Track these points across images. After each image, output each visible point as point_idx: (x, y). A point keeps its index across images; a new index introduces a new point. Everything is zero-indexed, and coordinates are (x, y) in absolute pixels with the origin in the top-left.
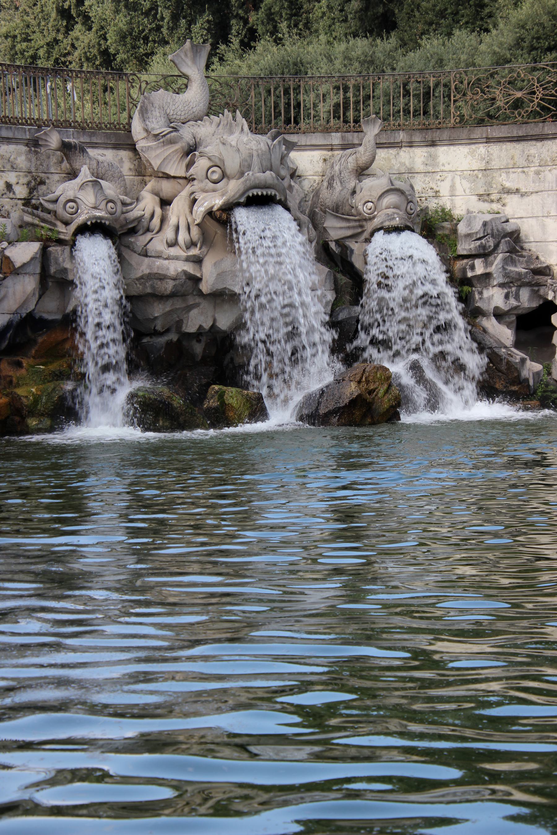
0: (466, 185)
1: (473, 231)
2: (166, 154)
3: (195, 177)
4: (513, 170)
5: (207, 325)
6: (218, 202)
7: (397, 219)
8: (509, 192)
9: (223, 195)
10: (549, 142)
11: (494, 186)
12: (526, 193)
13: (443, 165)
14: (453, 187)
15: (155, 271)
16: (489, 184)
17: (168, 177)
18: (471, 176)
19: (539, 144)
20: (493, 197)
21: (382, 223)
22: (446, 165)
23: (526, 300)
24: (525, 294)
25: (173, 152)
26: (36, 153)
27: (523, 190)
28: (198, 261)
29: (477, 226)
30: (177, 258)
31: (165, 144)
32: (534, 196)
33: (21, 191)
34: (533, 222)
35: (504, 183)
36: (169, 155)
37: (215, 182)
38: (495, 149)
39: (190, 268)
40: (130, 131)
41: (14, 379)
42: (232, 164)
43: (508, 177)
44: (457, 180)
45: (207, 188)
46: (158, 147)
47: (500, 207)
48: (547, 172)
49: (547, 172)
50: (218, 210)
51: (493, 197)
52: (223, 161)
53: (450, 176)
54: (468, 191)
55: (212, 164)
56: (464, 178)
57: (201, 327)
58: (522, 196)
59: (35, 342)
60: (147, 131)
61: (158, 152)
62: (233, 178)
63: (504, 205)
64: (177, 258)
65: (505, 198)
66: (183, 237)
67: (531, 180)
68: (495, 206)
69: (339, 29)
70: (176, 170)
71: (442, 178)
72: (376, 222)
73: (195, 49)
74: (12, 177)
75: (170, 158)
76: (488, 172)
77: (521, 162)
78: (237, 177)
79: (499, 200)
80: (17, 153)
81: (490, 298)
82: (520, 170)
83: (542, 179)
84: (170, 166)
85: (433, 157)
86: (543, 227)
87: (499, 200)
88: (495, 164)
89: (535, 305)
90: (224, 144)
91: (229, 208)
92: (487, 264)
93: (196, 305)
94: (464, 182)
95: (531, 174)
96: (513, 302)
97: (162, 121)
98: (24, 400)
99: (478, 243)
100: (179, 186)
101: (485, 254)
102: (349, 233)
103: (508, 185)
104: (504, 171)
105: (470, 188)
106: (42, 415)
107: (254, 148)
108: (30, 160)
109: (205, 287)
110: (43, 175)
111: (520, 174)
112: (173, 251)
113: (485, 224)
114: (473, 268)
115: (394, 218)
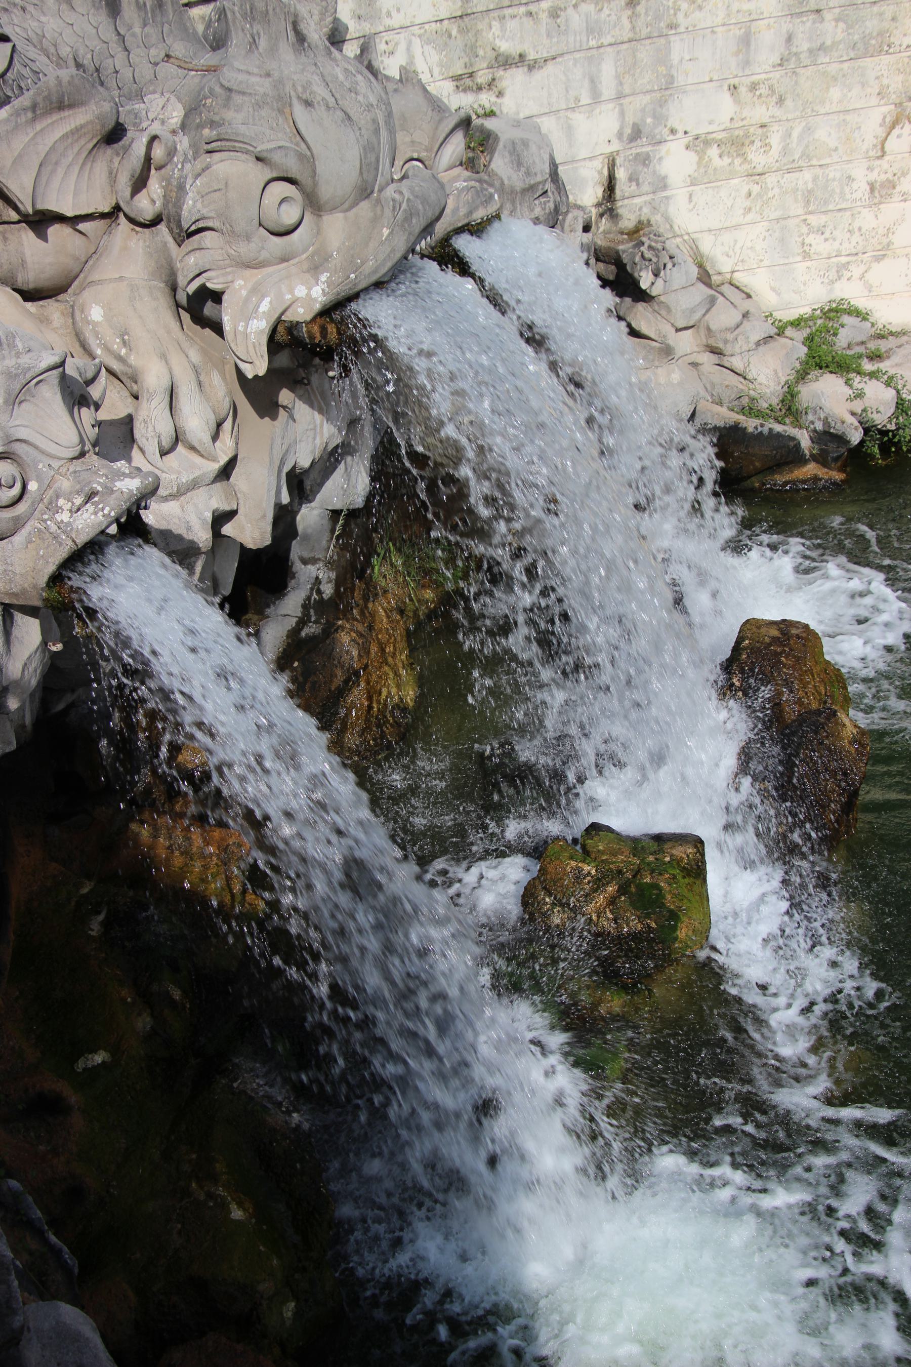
0: (434, 57)
1: (539, 178)
2: (43, 148)
3: (210, 224)
6: (306, 297)
7: (496, 196)
8: (505, 62)
9: (315, 269)
11: (481, 53)
12: (535, 61)
13: (389, 15)
16: (472, 50)
17: (40, 221)
21: (470, 213)
22: (394, 13)
25: (65, 137)
27: (532, 56)
32: (550, 67)
36: (53, 149)
45: (264, 255)
46: (17, 127)
47: (493, 99)
48: (570, 11)
49: (570, 11)
50: (314, 319)
51: (482, 78)
52: (308, 160)
53: (402, 37)
54: (436, 71)
55: (269, 176)
56: (429, 42)
58: (531, 68)
61: (19, 142)
62: (334, 209)
63: (500, 94)
65: (501, 78)
67: (543, 30)
68: (486, 99)
70: (75, 194)
71: (390, 48)
76: (466, 19)
78: (346, 205)
79: (491, 84)
82: (522, 10)
83: (563, 28)
86: (569, 130)
90: (308, 104)
95: (544, 16)
103: (504, 46)
104: (495, 14)
105: (441, 64)
107: (373, 99)
111: (525, 19)
115: (491, 196)
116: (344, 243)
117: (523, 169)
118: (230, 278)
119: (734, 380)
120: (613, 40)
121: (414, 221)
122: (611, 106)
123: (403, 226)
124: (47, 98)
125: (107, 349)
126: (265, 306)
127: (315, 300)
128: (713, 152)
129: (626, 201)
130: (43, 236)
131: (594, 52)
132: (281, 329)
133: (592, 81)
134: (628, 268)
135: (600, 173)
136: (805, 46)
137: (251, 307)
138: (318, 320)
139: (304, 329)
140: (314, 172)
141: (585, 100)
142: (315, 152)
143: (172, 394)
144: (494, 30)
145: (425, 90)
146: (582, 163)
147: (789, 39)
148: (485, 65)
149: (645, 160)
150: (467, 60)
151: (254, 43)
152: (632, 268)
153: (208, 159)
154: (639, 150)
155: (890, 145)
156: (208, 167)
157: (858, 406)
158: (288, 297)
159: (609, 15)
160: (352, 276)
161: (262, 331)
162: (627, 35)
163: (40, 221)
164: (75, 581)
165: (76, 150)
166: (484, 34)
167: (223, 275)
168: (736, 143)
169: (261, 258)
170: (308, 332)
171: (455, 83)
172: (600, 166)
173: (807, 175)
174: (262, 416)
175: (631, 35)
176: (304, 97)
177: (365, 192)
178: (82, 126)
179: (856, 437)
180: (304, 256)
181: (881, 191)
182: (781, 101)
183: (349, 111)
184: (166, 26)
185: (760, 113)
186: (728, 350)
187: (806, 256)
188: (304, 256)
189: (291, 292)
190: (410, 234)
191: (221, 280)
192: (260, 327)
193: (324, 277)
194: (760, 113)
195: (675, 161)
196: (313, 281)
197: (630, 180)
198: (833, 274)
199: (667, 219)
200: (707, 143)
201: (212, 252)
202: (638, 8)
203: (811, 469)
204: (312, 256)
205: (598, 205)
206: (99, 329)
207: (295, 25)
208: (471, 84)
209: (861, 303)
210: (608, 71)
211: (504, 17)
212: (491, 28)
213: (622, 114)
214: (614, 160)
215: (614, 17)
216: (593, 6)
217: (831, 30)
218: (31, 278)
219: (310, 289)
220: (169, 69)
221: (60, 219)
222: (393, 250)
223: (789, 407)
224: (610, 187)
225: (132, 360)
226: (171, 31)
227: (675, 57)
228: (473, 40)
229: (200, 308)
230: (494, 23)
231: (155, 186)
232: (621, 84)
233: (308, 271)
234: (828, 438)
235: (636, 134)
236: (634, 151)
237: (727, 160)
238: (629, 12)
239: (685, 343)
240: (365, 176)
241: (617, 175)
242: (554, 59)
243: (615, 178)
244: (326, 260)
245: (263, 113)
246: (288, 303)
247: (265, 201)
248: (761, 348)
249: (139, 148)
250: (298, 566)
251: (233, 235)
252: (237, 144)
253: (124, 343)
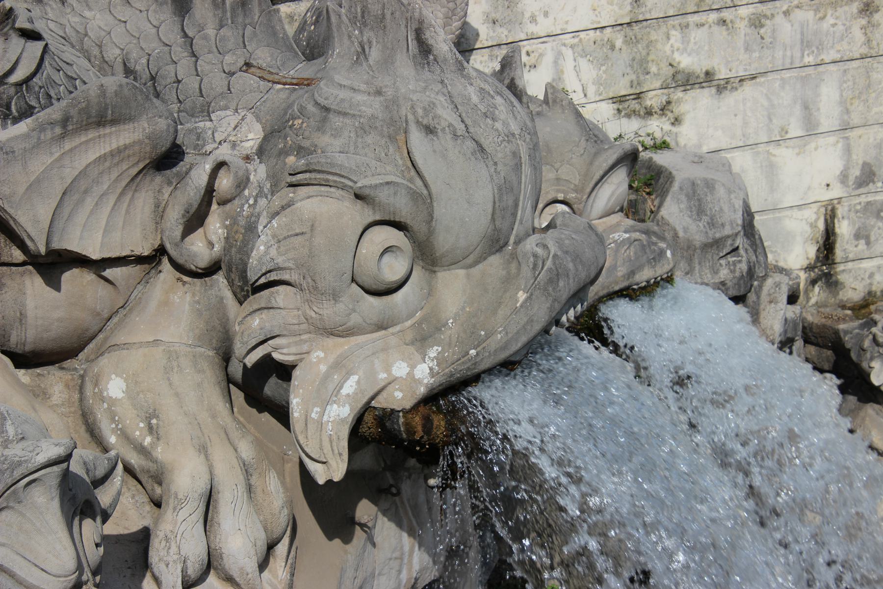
0: (589, 72)
1: (727, 231)
2: (70, 173)
3: (286, 277)
4: (696, 18)
6: (407, 375)
8: (686, 81)
9: (421, 341)
11: (653, 69)
12: (727, 81)
13: (533, 19)
16: (641, 66)
17: (53, 264)
18: (599, 42)
20: (653, 100)
21: (632, 273)
22: (540, 18)
25: (102, 159)
27: (722, 73)
31: (67, 126)
32: (748, 89)
35: (676, 56)
36: (83, 173)
43: (685, 40)
46: (38, 145)
47: (667, 127)
48: (779, 19)
49: (779, 19)
50: (415, 407)
51: (653, 100)
52: (424, 200)
53: (548, 49)
54: (591, 90)
55: (371, 219)
56: (584, 54)
58: (720, 89)
61: (39, 164)
62: (454, 263)
63: (677, 121)
65: (679, 101)
67: (740, 43)
68: (657, 127)
75: (83, 185)
76: (636, 27)
79: (664, 109)
82: (713, 16)
83: (768, 40)
84: (81, 217)
86: (771, 169)
90: (429, 130)
94: (583, 63)
95: (742, 26)
100: (103, 290)
103: (685, 62)
105: (598, 82)
107: (514, 127)
111: (716, 29)
115: (662, 253)
116: (463, 308)
117: (705, 219)
118: (305, 348)
120: (838, 57)
121: (561, 284)
122: (832, 139)
123: (545, 289)
124: (85, 111)
125: (125, 436)
126: (350, 387)
127: (419, 382)
129: (850, 265)
130: (54, 283)
131: (810, 71)
132: (369, 418)
133: (806, 107)
134: (853, 355)
135: (813, 226)
137: (331, 387)
138: (421, 409)
139: (401, 420)
140: (431, 216)
141: (795, 131)
142: (434, 190)
143: (209, 500)
144: (672, 41)
145: (579, 115)
146: (788, 213)
148: (658, 84)
150: (634, 77)
151: (363, 53)
152: (859, 356)
153: (290, 194)
154: (870, 198)
156: (289, 205)
158: (383, 376)
159: (834, 25)
160: (473, 352)
161: (343, 421)
162: (858, 49)
163: (53, 264)
165: (115, 174)
166: (659, 46)
167: (296, 343)
169: (349, 324)
170: (407, 424)
171: (616, 106)
172: (814, 217)
174: (330, 536)
175: (864, 50)
176: (425, 122)
177: (496, 243)
178: (126, 147)
180: (409, 323)
183: (482, 141)
184: (249, 29)
188: (409, 323)
189: (388, 369)
190: (555, 300)
191: (293, 350)
192: (340, 413)
193: (433, 352)
196: (418, 356)
197: (857, 236)
201: (283, 312)
202: (877, 17)
204: (419, 323)
205: (809, 268)
206: (118, 409)
207: (419, 34)
208: (637, 107)
211: (687, 26)
212: (668, 38)
213: (848, 150)
214: (833, 210)
215: (841, 28)
216: (809, 15)
218: (27, 337)
219: (413, 367)
220: (250, 80)
221: (81, 261)
222: (531, 321)
224: (828, 244)
225: (159, 452)
226: (255, 34)
228: (644, 53)
229: (261, 386)
230: (673, 32)
231: (215, 226)
232: (848, 112)
233: (412, 343)
235: (868, 177)
236: (864, 199)
238: (864, 22)
240: (498, 223)
241: (837, 230)
242: (753, 78)
243: (834, 234)
244: (438, 329)
245: (369, 139)
246: (383, 384)
247: (363, 249)
249: (200, 177)
251: (313, 290)
252: (331, 177)
253: (150, 428)
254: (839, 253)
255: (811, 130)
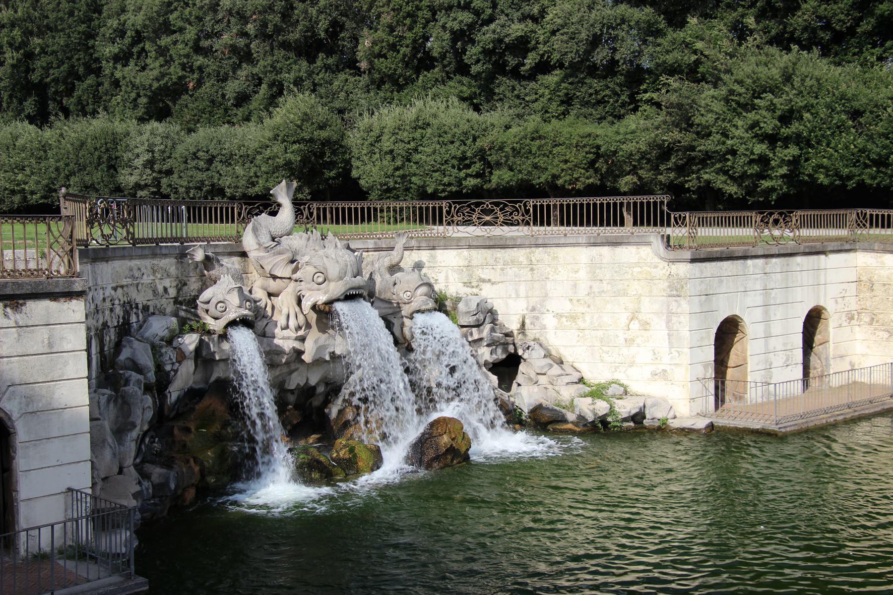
0: (456, 276)
5: (302, 384)
6: (322, 298)
8: (484, 281)
9: (325, 293)
10: (509, 251)
14: (447, 277)
15: (274, 348)
16: (471, 276)
17: (275, 277)
18: (459, 270)
19: (503, 251)
20: (473, 284)
23: (500, 355)
24: (499, 351)
26: (182, 262)
27: (493, 280)
28: (302, 339)
29: (473, 307)
30: (288, 338)
33: (172, 292)
34: (499, 301)
37: (319, 284)
38: (474, 252)
39: (297, 345)
40: (241, 241)
41: (188, 443)
42: (333, 271)
44: (450, 272)
51: (474, 284)
52: (326, 269)
57: (298, 384)
59: (193, 409)
60: (259, 244)
64: (288, 338)
66: (292, 323)
68: (475, 290)
69: (128, 113)
72: (414, 306)
73: (288, 186)
74: (167, 283)
77: (491, 262)
79: (477, 287)
80: (169, 264)
81: (483, 354)
85: (433, 257)
87: (477, 287)
88: (474, 263)
89: (504, 356)
91: (330, 303)
92: (480, 332)
93: (296, 370)
95: (499, 270)
96: (495, 356)
97: (269, 237)
98: (206, 463)
99: (475, 318)
101: (478, 326)
102: (390, 311)
103: (483, 276)
106: (219, 473)
108: (177, 269)
109: (307, 358)
110: (185, 279)
112: (286, 333)
113: (478, 305)
114: (471, 334)
119: (555, 394)
128: (564, 319)
136: (597, 290)
147: (591, 287)
149: (537, 318)
155: (631, 326)
157: (592, 407)
163: (275, 277)
164: (229, 329)
168: (573, 318)
173: (600, 333)
179: (590, 418)
181: (629, 342)
182: (589, 306)
185: (581, 309)
186: (555, 383)
187: (602, 361)
194: (581, 309)
195: (549, 320)
198: (613, 369)
199: (546, 339)
200: (561, 316)
203: (570, 426)
209: (625, 382)
210: (522, 289)
217: (605, 286)
218: (271, 290)
223: (571, 406)
224: (523, 324)
227: (548, 288)
234: (581, 418)
235: (533, 309)
237: (569, 323)
239: (543, 380)
248: (570, 386)
250: (343, 390)
254: (526, 327)
255: (518, 296)
